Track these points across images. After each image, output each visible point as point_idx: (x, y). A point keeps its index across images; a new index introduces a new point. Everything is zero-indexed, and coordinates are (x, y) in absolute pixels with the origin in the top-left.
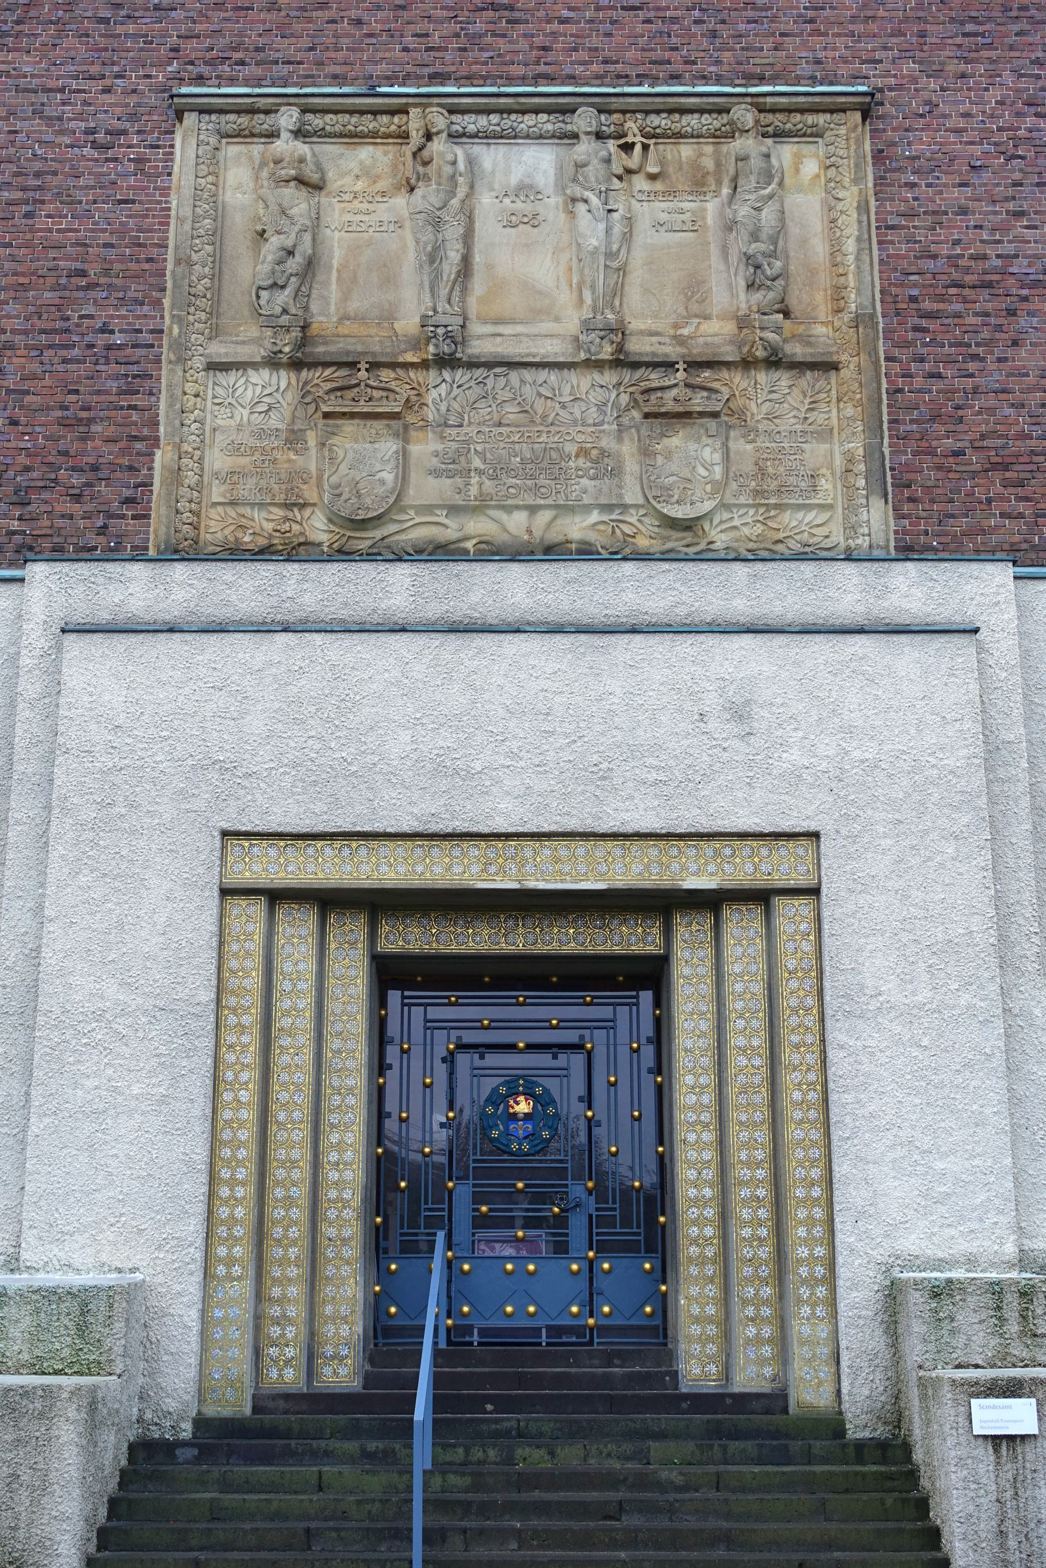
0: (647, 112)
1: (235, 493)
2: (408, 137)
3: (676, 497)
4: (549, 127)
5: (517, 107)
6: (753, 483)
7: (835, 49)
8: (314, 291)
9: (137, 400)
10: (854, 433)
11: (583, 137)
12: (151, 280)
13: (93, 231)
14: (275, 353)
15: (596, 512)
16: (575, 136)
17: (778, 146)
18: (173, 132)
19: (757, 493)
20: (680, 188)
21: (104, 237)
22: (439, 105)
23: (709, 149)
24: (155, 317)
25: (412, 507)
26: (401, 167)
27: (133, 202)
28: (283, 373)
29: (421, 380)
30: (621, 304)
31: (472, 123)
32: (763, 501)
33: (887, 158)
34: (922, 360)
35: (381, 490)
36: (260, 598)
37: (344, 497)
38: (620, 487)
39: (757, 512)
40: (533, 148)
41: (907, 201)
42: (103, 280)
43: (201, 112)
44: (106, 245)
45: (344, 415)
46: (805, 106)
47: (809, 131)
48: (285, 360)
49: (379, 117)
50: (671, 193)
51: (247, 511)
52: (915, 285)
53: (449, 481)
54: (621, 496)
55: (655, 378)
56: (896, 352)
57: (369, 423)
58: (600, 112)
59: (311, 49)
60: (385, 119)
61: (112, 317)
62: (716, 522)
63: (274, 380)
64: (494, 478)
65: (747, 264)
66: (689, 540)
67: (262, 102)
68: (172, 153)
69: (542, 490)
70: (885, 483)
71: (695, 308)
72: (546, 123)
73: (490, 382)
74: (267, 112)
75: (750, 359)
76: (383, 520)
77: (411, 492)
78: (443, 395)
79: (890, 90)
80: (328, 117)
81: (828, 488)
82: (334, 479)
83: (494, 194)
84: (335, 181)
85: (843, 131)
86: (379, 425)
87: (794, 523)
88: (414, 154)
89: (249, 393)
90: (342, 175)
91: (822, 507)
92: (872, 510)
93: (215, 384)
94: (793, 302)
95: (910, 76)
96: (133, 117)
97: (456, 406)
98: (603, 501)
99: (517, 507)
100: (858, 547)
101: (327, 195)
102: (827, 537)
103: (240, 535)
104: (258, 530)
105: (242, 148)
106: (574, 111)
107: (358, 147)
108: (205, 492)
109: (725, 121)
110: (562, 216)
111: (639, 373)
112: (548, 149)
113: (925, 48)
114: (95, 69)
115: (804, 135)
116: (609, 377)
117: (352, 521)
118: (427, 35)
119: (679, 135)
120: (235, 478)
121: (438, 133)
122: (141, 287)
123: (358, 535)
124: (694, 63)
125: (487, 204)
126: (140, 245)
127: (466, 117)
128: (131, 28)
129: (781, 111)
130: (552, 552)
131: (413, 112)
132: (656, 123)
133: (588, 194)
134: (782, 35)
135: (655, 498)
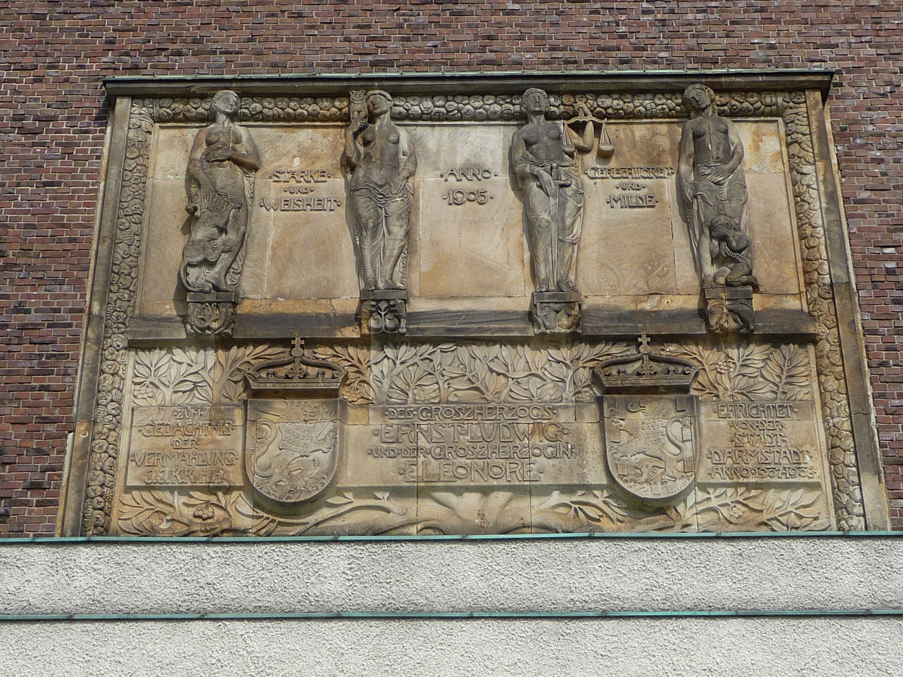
1: (154, 475)
3: (645, 476)
4: (497, 108)
5: (462, 89)
7: (788, 36)
8: (246, 269)
13: (14, 212)
14: (202, 330)
17: (736, 125)
19: (735, 471)
20: (635, 165)
21: (25, 219)
22: (381, 88)
23: (664, 129)
25: (349, 489)
27: (58, 184)
31: (415, 106)
32: (741, 480)
35: (315, 471)
36: (175, 585)
37: (274, 479)
38: (582, 466)
40: (479, 129)
42: (20, 261)
44: (27, 226)
50: (625, 171)
51: (166, 496)
52: (890, 258)
54: (583, 476)
59: (250, 40)
61: (29, 296)
65: (712, 237)
67: (196, 87)
68: (102, 138)
71: (656, 283)
73: (437, 357)
77: (349, 474)
79: (849, 71)
82: (263, 460)
83: (439, 173)
84: (270, 161)
85: (802, 109)
89: (173, 372)
90: (279, 157)
94: (760, 273)
95: (867, 59)
96: (63, 104)
99: (468, 489)
101: (263, 176)
102: (816, 519)
107: (296, 130)
113: (882, 33)
114: (28, 61)
116: (565, 353)
117: (283, 505)
118: (369, 27)
124: (645, 49)
126: (63, 226)
128: (67, 23)
130: (509, 533)
131: (356, 95)
134: (733, 23)
135: (622, 476)
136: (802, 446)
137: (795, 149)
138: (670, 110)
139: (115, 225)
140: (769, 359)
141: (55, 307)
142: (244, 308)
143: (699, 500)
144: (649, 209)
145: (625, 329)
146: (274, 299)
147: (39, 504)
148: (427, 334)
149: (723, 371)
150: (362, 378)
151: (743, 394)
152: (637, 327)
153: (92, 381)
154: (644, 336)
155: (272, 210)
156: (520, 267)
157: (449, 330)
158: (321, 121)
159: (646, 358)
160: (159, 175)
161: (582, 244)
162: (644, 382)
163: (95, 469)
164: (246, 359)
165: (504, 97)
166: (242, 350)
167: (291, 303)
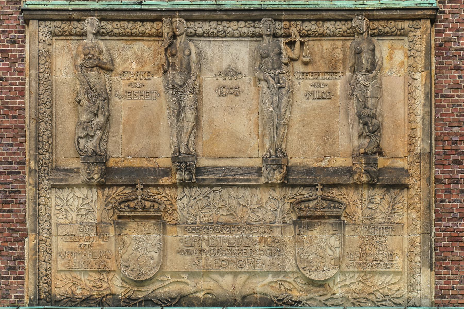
0: (303, 21)
1: (70, 264)
2: (162, 36)
3: (315, 267)
4: (246, 30)
6: (358, 259)
8: (110, 138)
9: (12, 207)
10: (415, 229)
11: (265, 37)
12: (17, 130)
15: (270, 276)
16: (261, 36)
17: (380, 42)
18: (23, 32)
19: (360, 265)
22: (180, 16)
23: (339, 44)
24: (19, 154)
26: (158, 56)
28: (94, 190)
29: (172, 194)
30: (286, 147)
32: (362, 270)
33: (445, 49)
34: (457, 182)
35: (151, 263)
37: (131, 267)
38: (284, 261)
39: (359, 276)
40: (236, 43)
41: (454, 78)
43: (39, 20)
45: (129, 217)
46: (397, 17)
47: (399, 32)
48: (95, 183)
49: (145, 23)
51: (78, 275)
52: (456, 134)
53: (189, 257)
54: (284, 266)
55: (305, 193)
56: (442, 177)
57: (144, 222)
58: (275, 20)
60: (148, 25)
62: (337, 281)
63: (90, 195)
64: (214, 255)
65: (359, 122)
66: (321, 293)
67: (75, 15)
68: (23, 46)
69: (241, 263)
70: (431, 258)
71: (328, 149)
72: (243, 27)
73: (211, 196)
74: (79, 20)
75: (358, 183)
76: (153, 280)
77: (168, 264)
78: (185, 204)
80: (115, 24)
81: (400, 262)
82: (125, 256)
83: (213, 74)
84: (120, 67)
85: (418, 33)
86: (150, 223)
87: (380, 283)
88: (166, 50)
89: (76, 203)
90: (124, 61)
91: (396, 273)
92: (423, 276)
93: (56, 197)
94: (384, 145)
97: (192, 211)
98: (274, 269)
99: (227, 273)
100: (414, 297)
101: (116, 76)
102: (398, 291)
103: (74, 289)
104: (84, 286)
105: (65, 43)
106: (260, 20)
107: (133, 42)
108: (53, 264)
109: (349, 26)
110: (253, 89)
111: (296, 191)
112: (244, 44)
115: (396, 35)
116: (279, 193)
117: (136, 281)
119: (322, 35)
120: (70, 255)
121: (179, 35)
122: (11, 135)
123: (139, 289)
125: (209, 81)
126: (8, 108)
127: (196, 24)
129: (382, 20)
132: (308, 28)
133: (268, 76)
135: (303, 268)
136: (395, 250)
137: (411, 60)
138: (344, 32)
139: (38, 111)
140: (383, 198)
141: (10, 161)
142: (111, 163)
143: (341, 280)
144: (328, 101)
145: (310, 179)
146: (126, 157)
147: (15, 278)
148: (207, 182)
149: (359, 206)
150: (173, 208)
151: (368, 219)
152: (315, 179)
153: (34, 210)
154: (319, 185)
155: (122, 99)
156: (256, 138)
157: (218, 180)
158: (147, 37)
159: (319, 198)
160: (58, 74)
161: (290, 124)
162: (318, 213)
163: (41, 261)
164: (113, 196)
165: (250, 22)
166: (111, 190)
167: (135, 160)
